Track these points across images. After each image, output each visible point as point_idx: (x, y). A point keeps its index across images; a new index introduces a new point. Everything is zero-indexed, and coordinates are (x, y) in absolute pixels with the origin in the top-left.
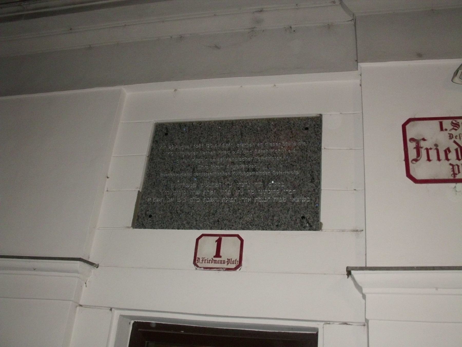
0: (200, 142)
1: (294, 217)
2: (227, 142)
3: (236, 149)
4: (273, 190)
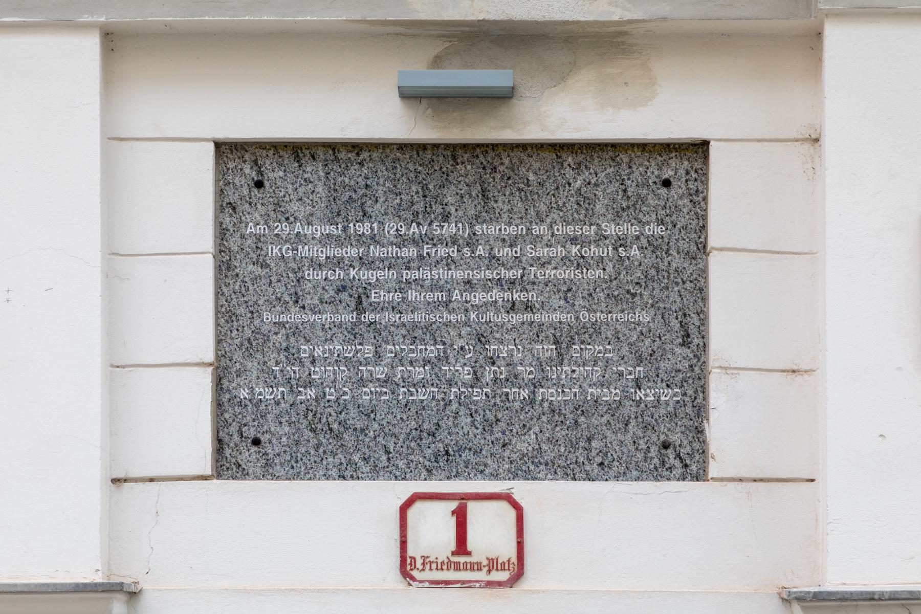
0: (365, 215)
1: (641, 442)
2: (446, 217)
3: (471, 243)
4: (584, 365)
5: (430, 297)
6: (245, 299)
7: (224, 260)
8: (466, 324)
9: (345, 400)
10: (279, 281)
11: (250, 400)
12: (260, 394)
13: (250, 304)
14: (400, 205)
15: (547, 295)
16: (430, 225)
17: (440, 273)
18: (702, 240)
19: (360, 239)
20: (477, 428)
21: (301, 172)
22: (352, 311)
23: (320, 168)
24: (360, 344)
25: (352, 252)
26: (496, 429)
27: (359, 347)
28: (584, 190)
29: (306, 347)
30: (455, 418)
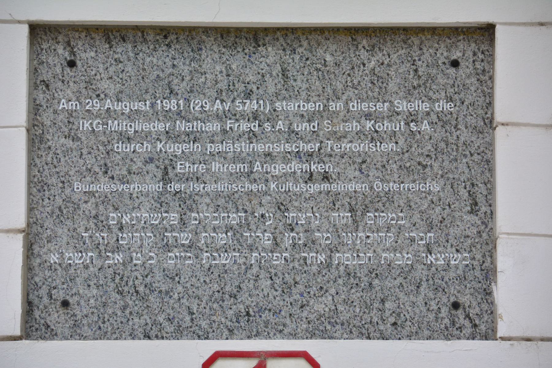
0: (171, 92)
1: (433, 303)
2: (248, 95)
4: (378, 231)
5: (232, 168)
6: (57, 170)
7: (37, 133)
8: (266, 193)
9: (151, 264)
10: (90, 153)
11: (60, 264)
12: (70, 259)
13: (62, 174)
14: (205, 83)
15: (342, 166)
16: (233, 101)
17: (243, 147)
18: (489, 115)
19: (167, 115)
20: (276, 290)
21: (111, 53)
22: (159, 182)
23: (130, 49)
24: (166, 212)
25: (160, 127)
26: (294, 291)
27: (165, 215)
28: (377, 70)
29: (115, 215)
30: (256, 281)
